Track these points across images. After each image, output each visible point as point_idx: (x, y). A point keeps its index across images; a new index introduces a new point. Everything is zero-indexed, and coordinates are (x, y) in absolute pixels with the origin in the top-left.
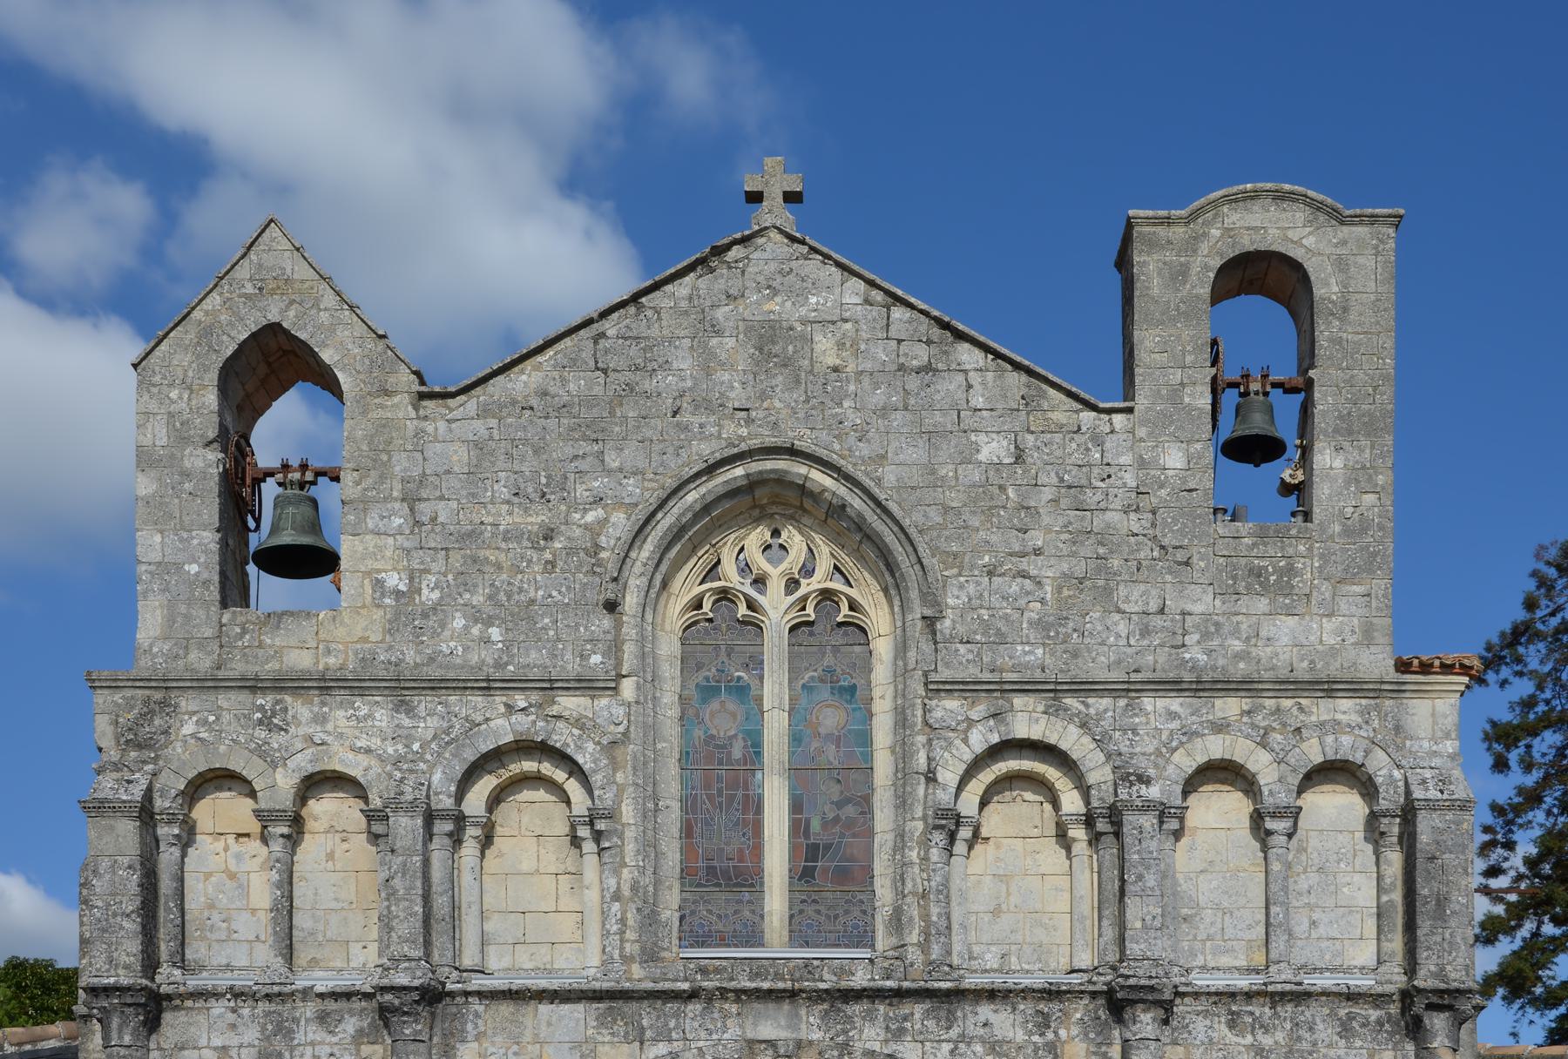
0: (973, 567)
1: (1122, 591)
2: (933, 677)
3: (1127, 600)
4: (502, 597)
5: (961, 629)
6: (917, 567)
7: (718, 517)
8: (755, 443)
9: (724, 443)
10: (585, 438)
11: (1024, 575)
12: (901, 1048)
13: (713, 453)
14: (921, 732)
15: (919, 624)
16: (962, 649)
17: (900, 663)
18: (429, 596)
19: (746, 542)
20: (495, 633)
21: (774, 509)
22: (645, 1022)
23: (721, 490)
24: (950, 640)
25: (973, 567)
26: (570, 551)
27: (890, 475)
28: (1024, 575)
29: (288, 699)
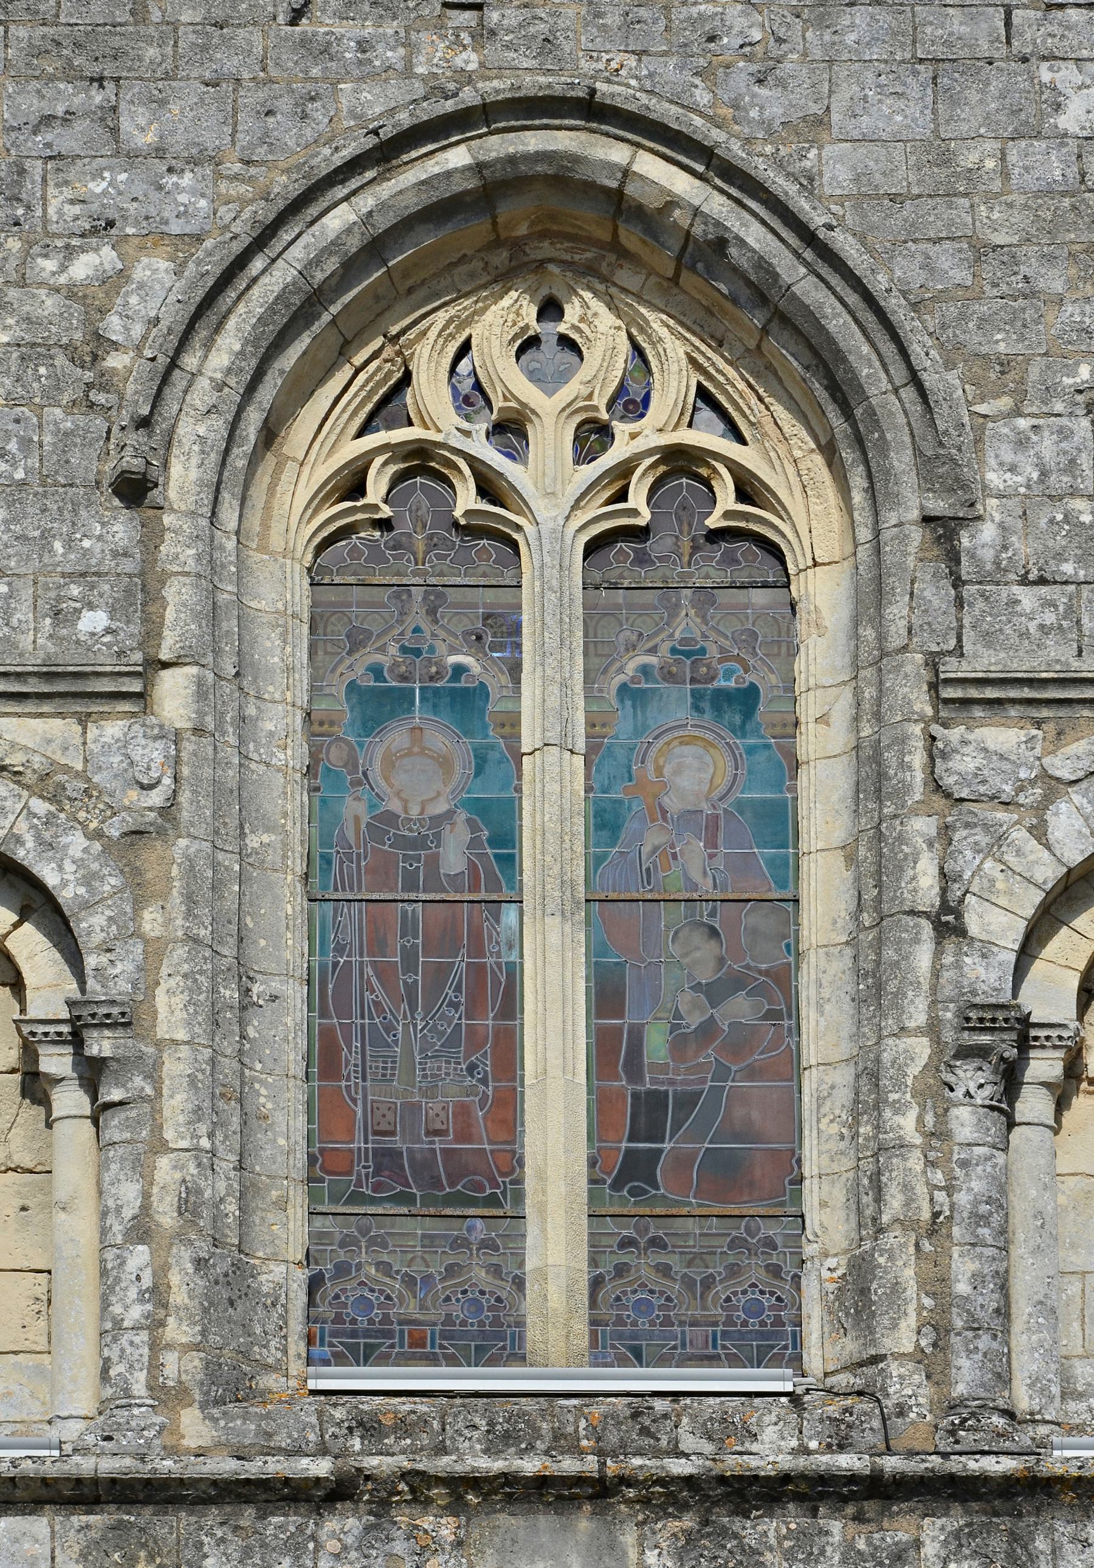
0: (1049, 391)
2: (952, 668)
5: (1022, 548)
6: (909, 394)
7: (406, 270)
8: (497, 87)
9: (419, 89)
10: (71, 75)
13: (392, 111)
15: (917, 535)
16: (1027, 598)
17: (868, 633)
19: (477, 331)
21: (545, 249)
23: (413, 203)
24: (996, 575)
25: (1049, 391)
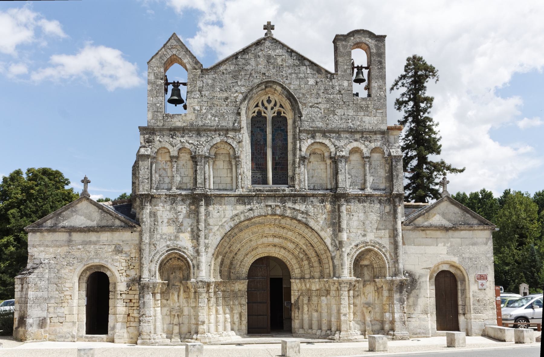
1: (337, 111)
3: (338, 113)
4: (218, 111)
11: (318, 107)
14: (298, 140)
16: (306, 123)
18: (204, 111)
20: (217, 119)
22: (246, 201)
26: (231, 102)
27: (292, 87)
28: (318, 107)
29: (176, 132)
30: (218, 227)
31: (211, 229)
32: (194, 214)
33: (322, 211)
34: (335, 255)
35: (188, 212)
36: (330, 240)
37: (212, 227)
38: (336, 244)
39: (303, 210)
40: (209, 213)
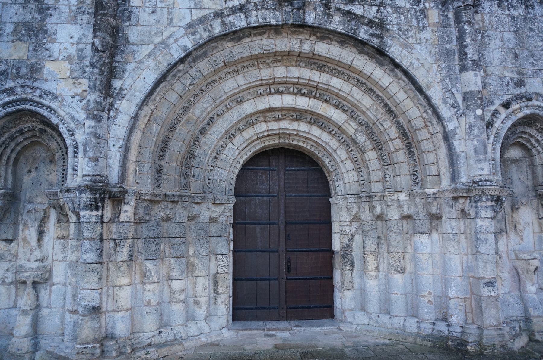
12: (353, 8)
30: (151, 47)
31: (133, 53)
32: (89, 13)
33: (418, 22)
34: (456, 128)
35: (74, 8)
36: (441, 93)
37: (135, 48)
38: (456, 102)
39: (371, 17)
40: (130, 12)
